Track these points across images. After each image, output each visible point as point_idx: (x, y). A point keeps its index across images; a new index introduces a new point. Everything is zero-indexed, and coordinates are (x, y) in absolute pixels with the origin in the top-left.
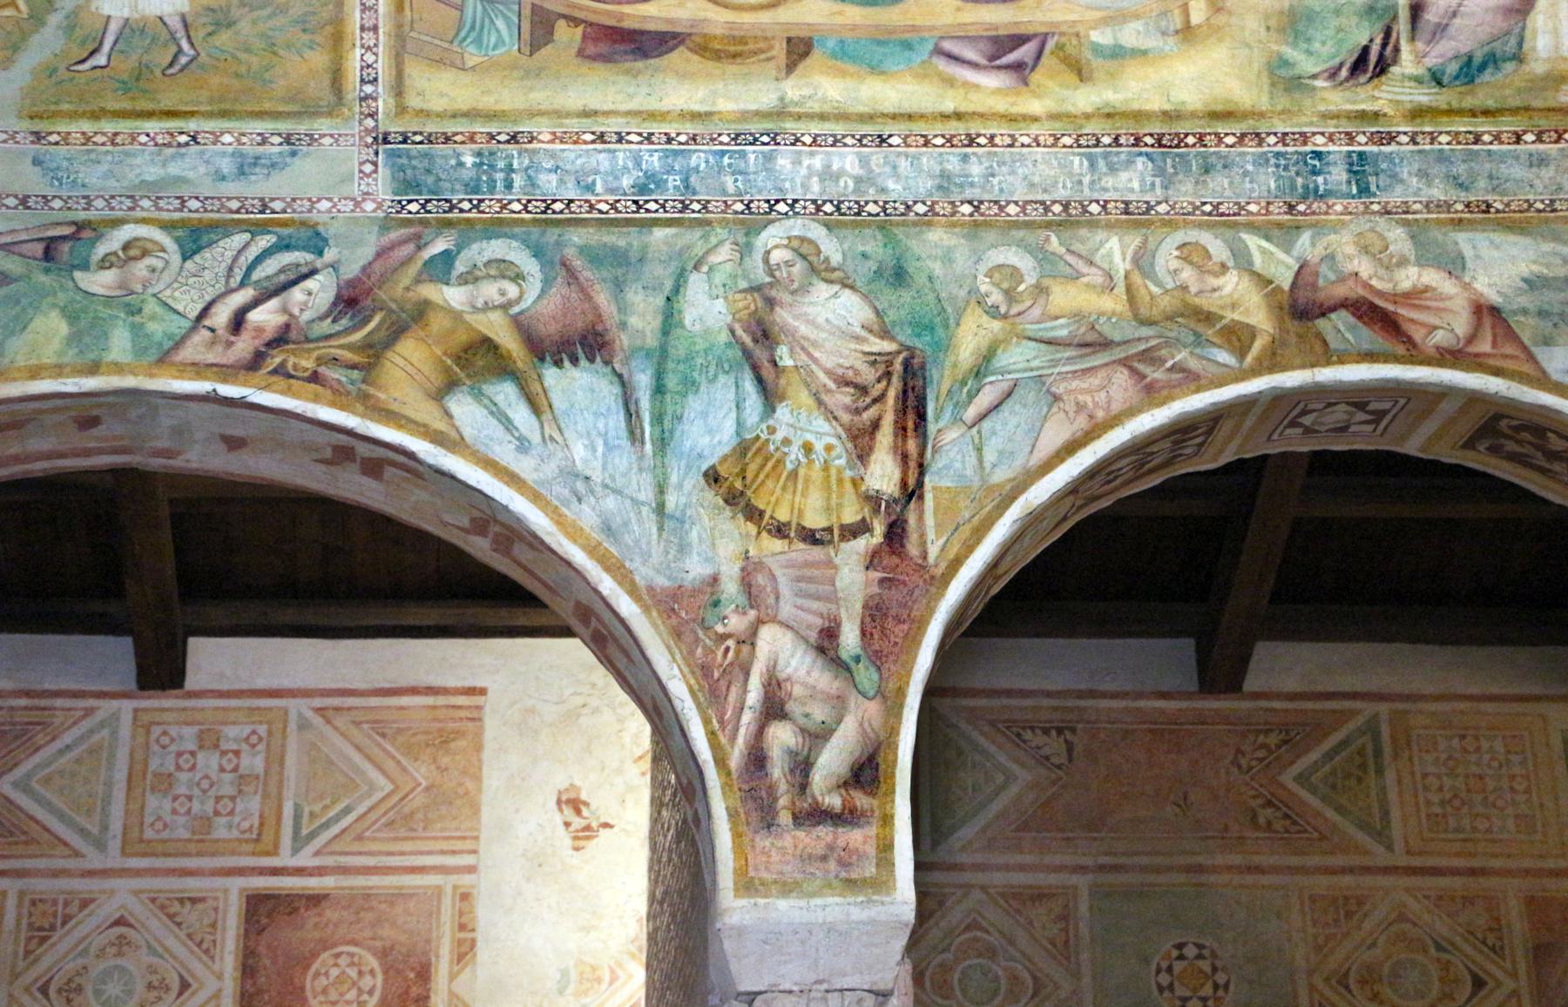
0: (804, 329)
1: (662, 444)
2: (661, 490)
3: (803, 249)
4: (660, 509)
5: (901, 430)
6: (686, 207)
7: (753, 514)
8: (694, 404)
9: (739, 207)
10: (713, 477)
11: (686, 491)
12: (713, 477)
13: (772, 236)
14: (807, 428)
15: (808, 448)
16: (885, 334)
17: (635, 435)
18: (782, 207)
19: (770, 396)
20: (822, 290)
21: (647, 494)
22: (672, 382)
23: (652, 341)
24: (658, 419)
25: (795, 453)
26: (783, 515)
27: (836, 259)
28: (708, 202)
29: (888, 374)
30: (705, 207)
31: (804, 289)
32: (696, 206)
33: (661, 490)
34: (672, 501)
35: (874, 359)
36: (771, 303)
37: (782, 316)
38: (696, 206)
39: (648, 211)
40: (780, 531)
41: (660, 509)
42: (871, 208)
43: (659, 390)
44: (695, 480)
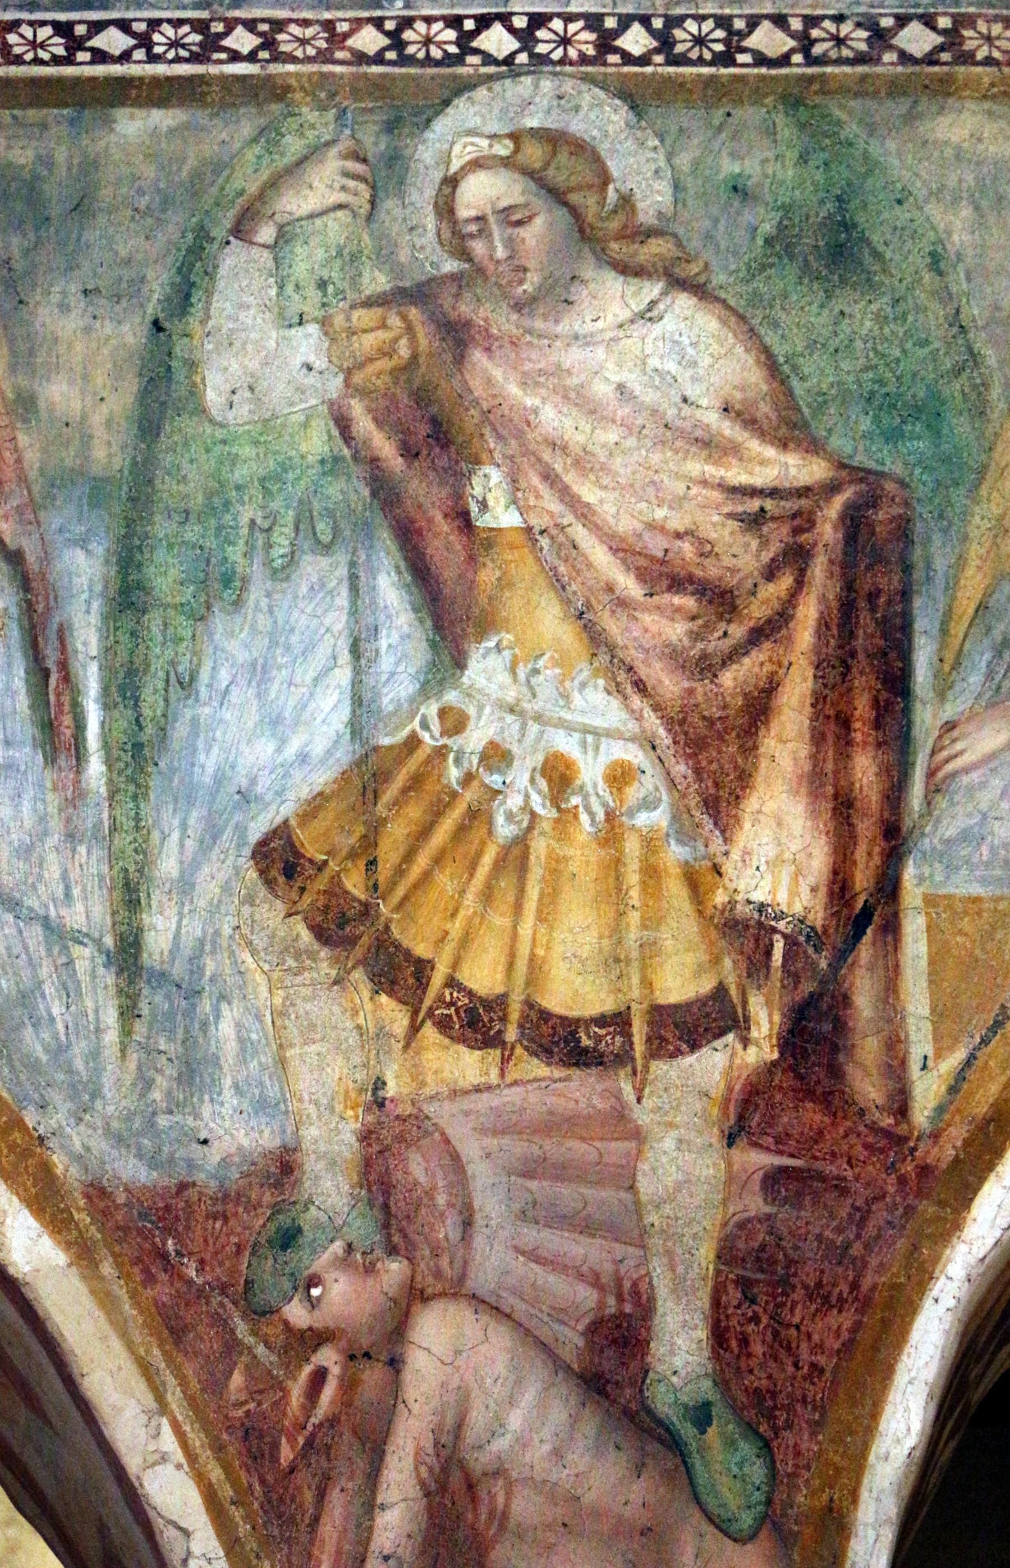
0: (552, 418)
1: (137, 756)
2: (130, 895)
3: (558, 170)
4: (127, 954)
5: (831, 726)
6: (211, 44)
7: (398, 972)
8: (231, 644)
9: (369, 40)
10: (280, 860)
11: (203, 903)
12: (280, 860)
13: (463, 132)
14: (556, 716)
15: (559, 776)
16: (791, 430)
17: (56, 735)
18: (497, 41)
19: (452, 624)
20: (610, 299)
21: (89, 911)
22: (166, 575)
23: (108, 452)
24: (124, 687)
25: (521, 789)
26: (483, 976)
27: (653, 199)
28: (279, 25)
29: (797, 557)
30: (269, 43)
31: (557, 294)
32: (243, 41)
33: (130, 895)
34: (162, 930)
35: (756, 510)
36: (458, 336)
37: (494, 377)
38: (243, 41)
39: (100, 56)
40: (475, 1022)
41: (127, 954)
42: (766, 39)
43: (128, 598)
44: (228, 869)
